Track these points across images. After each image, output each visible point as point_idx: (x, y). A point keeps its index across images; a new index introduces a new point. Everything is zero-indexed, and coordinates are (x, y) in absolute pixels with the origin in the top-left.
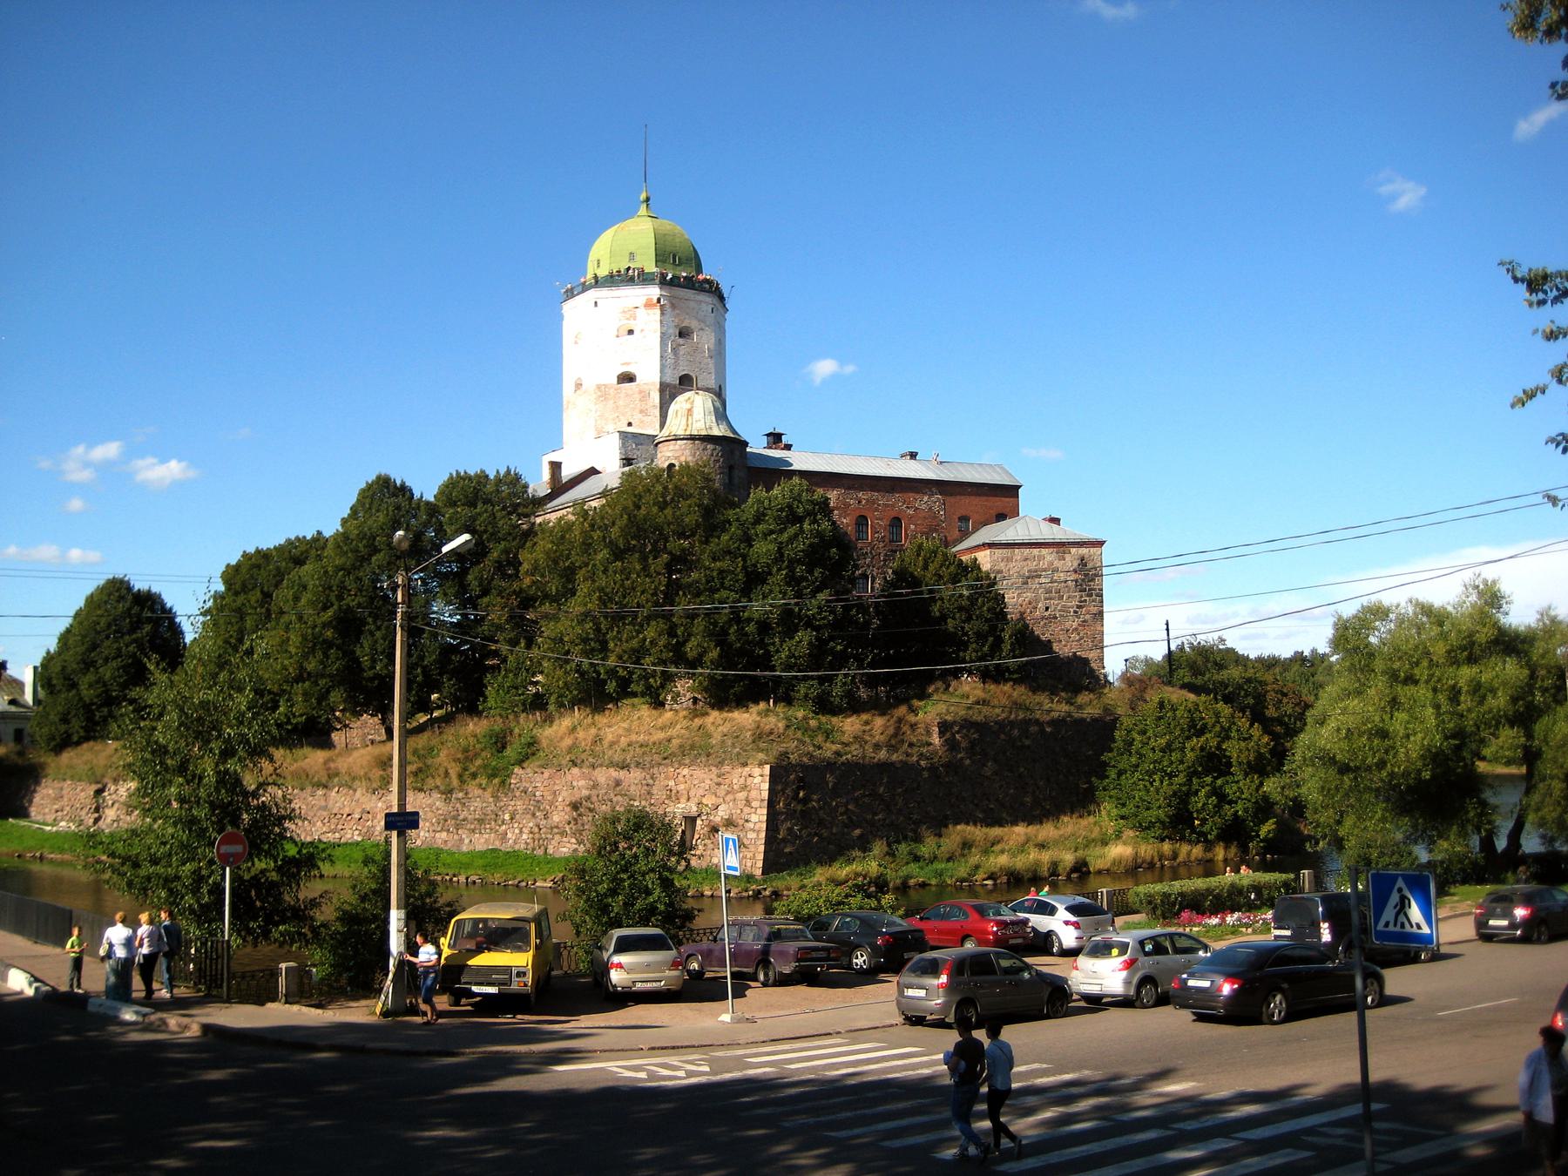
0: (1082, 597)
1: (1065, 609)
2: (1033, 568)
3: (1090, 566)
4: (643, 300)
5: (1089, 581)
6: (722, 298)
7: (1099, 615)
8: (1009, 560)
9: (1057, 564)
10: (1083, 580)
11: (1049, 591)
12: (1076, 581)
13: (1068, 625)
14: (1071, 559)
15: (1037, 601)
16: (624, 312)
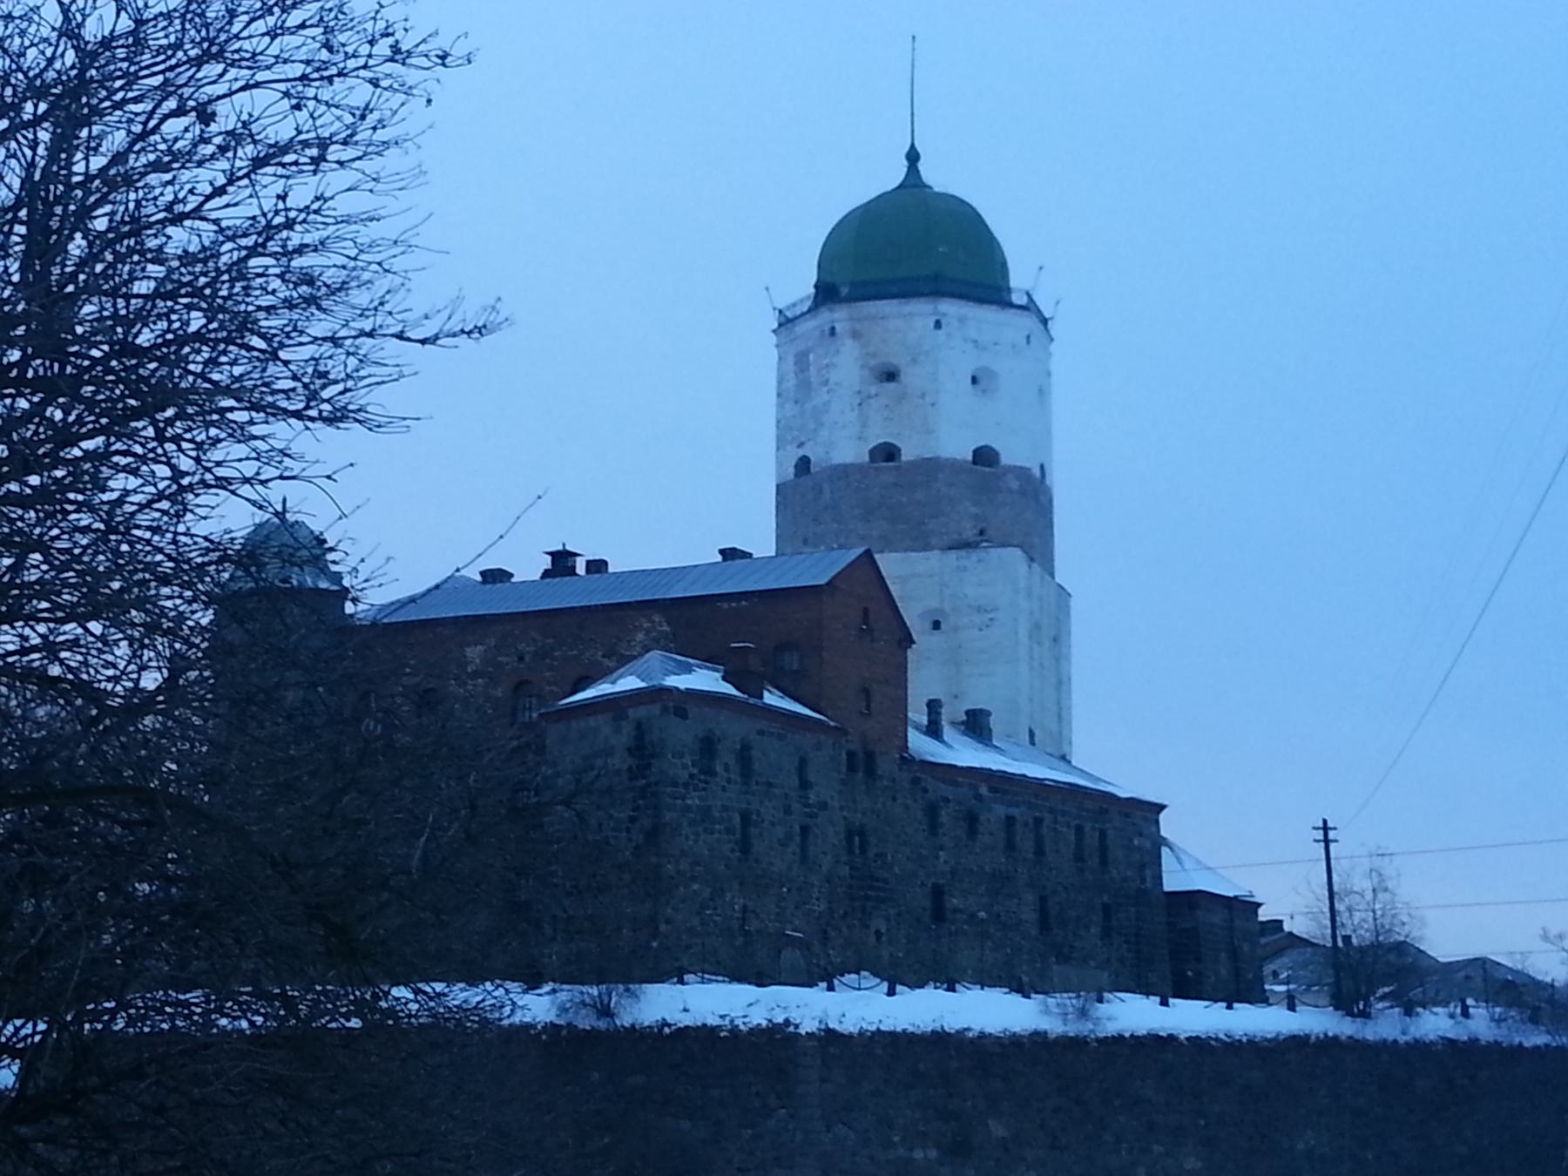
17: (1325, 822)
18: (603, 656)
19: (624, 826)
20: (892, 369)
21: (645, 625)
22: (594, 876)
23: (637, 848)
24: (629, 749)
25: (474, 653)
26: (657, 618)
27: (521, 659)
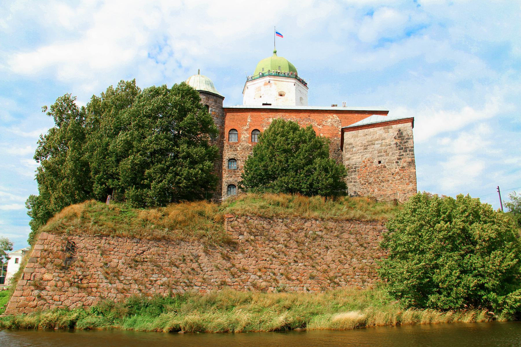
1: (390, 162)
2: (370, 139)
3: (404, 134)
4: (263, 83)
6: (305, 84)
7: (412, 163)
8: (356, 136)
9: (385, 135)
10: (401, 143)
12: (396, 144)
13: (393, 171)
15: (373, 159)
16: (257, 89)
18: (318, 125)
19: (395, 161)
20: (282, 94)
21: (331, 117)
22: (378, 178)
23: (403, 167)
24: (395, 138)
26: (335, 115)
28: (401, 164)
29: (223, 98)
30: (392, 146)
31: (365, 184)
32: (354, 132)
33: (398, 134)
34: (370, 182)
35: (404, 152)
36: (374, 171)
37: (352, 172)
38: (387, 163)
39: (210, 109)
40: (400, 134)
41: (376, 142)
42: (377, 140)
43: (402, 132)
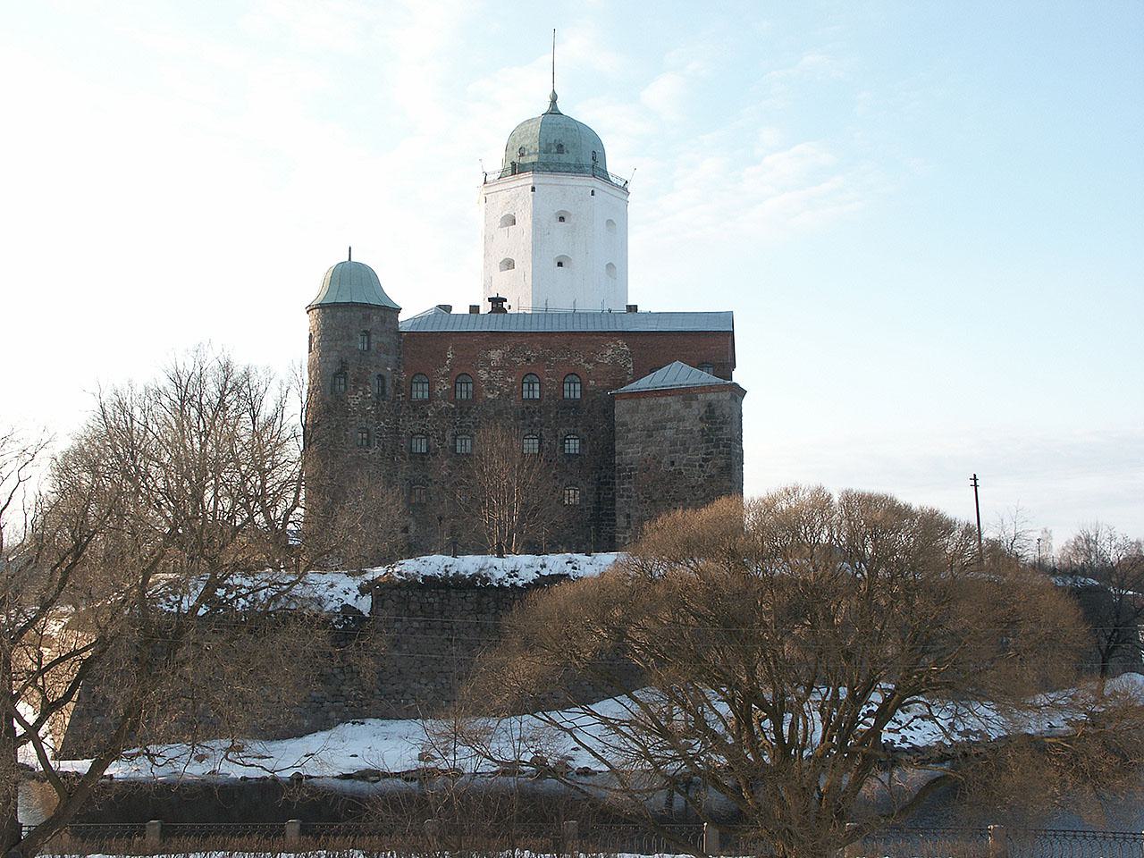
0: (708, 448)
1: (690, 464)
5: (717, 429)
9: (684, 412)
10: (710, 429)
11: (673, 444)
14: (697, 408)
17: (975, 475)
25: (495, 355)
27: (528, 360)
28: (708, 470)
29: (399, 310)
30: (697, 435)
31: (646, 502)
32: (631, 403)
33: (706, 412)
34: (654, 498)
35: (714, 447)
36: (664, 480)
37: (624, 477)
38: (685, 465)
39: (373, 337)
40: (710, 413)
41: (669, 425)
42: (670, 420)
43: (713, 409)
